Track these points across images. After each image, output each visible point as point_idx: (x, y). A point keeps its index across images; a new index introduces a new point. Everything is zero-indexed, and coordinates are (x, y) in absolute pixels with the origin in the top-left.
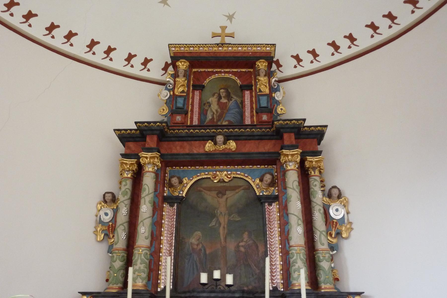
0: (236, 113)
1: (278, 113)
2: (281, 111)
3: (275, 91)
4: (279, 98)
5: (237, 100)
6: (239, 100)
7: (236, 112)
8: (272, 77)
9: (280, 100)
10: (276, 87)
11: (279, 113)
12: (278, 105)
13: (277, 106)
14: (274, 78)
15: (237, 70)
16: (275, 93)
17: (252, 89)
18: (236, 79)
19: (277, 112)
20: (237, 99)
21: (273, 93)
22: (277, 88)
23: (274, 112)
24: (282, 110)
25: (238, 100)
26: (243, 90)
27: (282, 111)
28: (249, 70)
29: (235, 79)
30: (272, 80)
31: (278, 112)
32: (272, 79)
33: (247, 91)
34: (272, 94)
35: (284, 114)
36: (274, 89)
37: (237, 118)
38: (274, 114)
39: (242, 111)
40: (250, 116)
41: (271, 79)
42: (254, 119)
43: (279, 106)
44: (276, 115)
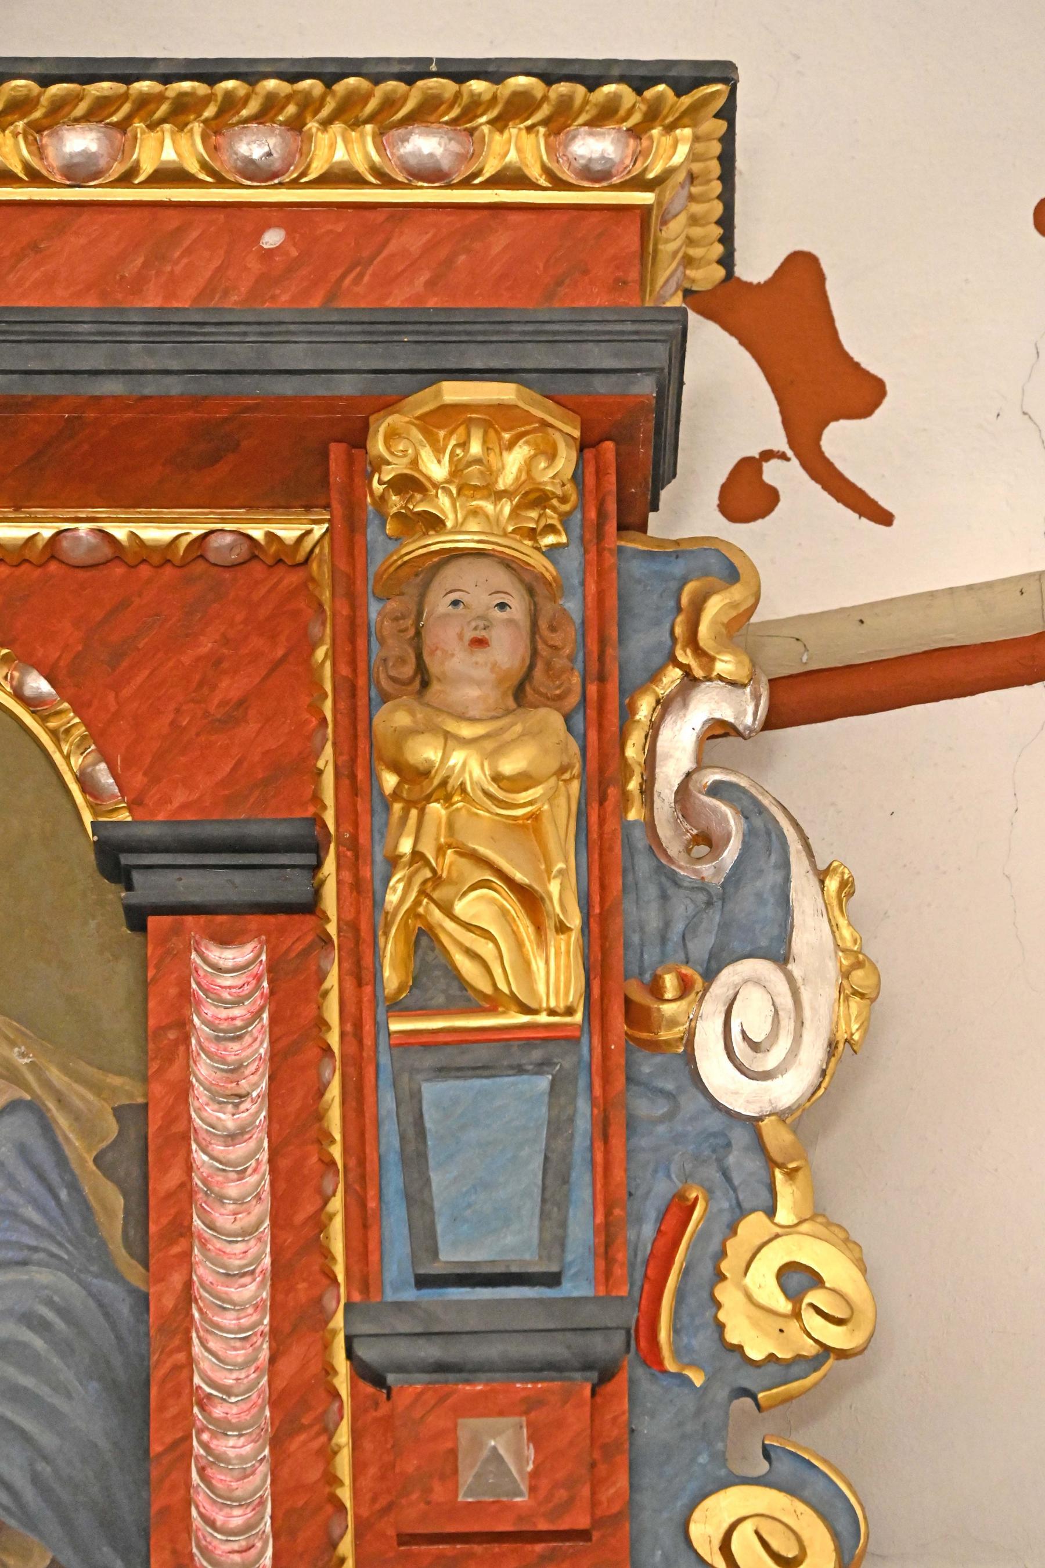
0: (38, 1343)
1: (739, 1349)
2: (784, 1306)
3: (701, 946)
4: (766, 1076)
5: (62, 1121)
6: (81, 1095)
7: (30, 1320)
8: (674, 674)
9: (782, 1116)
10: (730, 854)
11: (755, 1354)
12: (741, 1212)
13: (732, 1230)
14: (690, 681)
15: (47, 532)
16: (710, 976)
17: (311, 907)
18: (32, 704)
19: (721, 1327)
20: (55, 1074)
21: (670, 982)
22: (736, 875)
23: (676, 1330)
24: (814, 1297)
25: (61, 1100)
26: (153, 922)
27: (797, 1315)
28: (257, 533)
29: (18, 695)
30: (655, 728)
31: (732, 1337)
32: (664, 706)
33: (225, 941)
34: (656, 990)
35: (842, 1354)
36: (682, 908)
37: (47, 1440)
38: (670, 1366)
39: (142, 1301)
40: (274, 1403)
41: (644, 708)
42: (329, 1454)
43: (753, 1226)
44: (698, 1379)
